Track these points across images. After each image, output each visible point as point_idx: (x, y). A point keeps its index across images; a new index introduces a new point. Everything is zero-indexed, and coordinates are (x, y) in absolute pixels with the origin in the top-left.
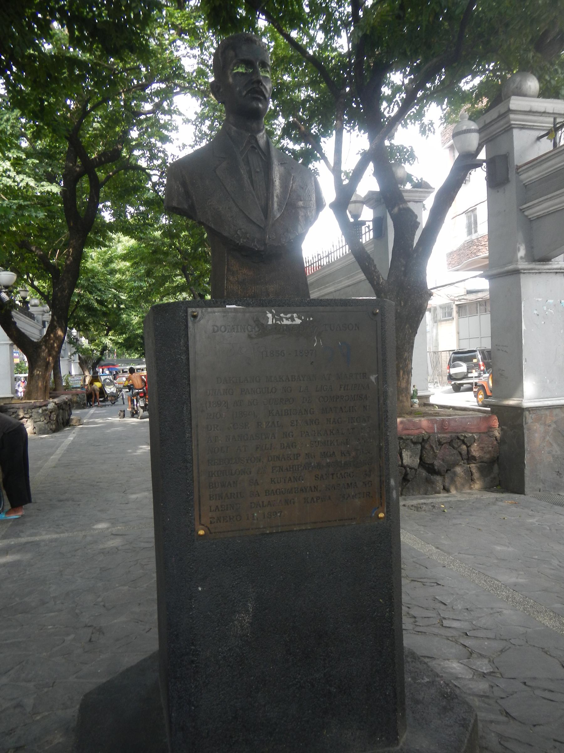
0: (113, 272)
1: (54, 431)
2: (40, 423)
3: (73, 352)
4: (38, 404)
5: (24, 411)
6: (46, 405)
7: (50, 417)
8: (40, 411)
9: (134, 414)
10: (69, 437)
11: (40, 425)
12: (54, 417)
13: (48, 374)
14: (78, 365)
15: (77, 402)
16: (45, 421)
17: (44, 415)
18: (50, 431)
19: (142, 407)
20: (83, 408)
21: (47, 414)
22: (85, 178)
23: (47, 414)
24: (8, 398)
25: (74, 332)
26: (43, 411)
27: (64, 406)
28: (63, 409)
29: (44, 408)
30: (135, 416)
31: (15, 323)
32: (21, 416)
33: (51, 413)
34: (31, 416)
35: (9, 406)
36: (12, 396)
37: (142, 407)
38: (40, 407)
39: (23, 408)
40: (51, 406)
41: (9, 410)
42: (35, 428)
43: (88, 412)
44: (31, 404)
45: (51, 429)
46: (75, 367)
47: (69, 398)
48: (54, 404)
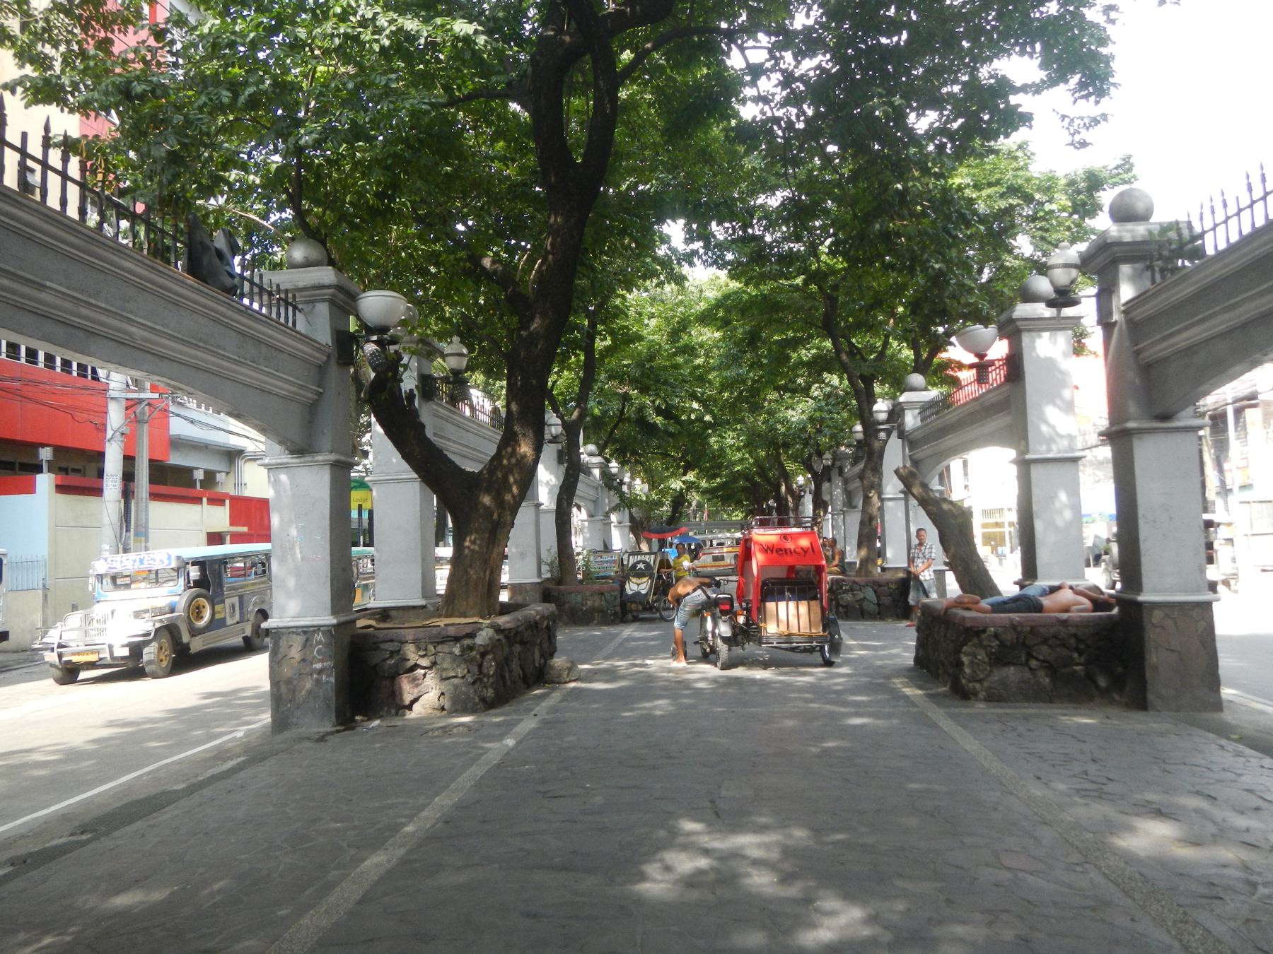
0: (689, 350)
1: (489, 705)
2: (456, 681)
3: (613, 504)
4: (452, 631)
5: (419, 649)
6: (472, 635)
7: (480, 666)
8: (457, 650)
9: (708, 656)
10: (517, 730)
11: (456, 687)
12: (491, 666)
13: (496, 550)
14: (627, 530)
15: (600, 611)
16: (470, 680)
17: (466, 661)
18: (481, 705)
19: (725, 640)
20: (612, 623)
21: (472, 660)
22: (587, 63)
23: (474, 658)
24: (414, 607)
25: (614, 466)
26: (463, 650)
27: (527, 635)
28: (522, 643)
29: (467, 642)
30: (712, 657)
31: (423, 426)
32: (412, 663)
33: (483, 655)
34: (434, 664)
35: (381, 634)
36: (422, 602)
37: (725, 640)
38: (457, 639)
39: (416, 642)
40: (483, 637)
41: (384, 646)
42: (442, 694)
43: (617, 635)
44: (435, 631)
45: (483, 700)
46: (622, 536)
47: (546, 613)
48: (490, 632)
